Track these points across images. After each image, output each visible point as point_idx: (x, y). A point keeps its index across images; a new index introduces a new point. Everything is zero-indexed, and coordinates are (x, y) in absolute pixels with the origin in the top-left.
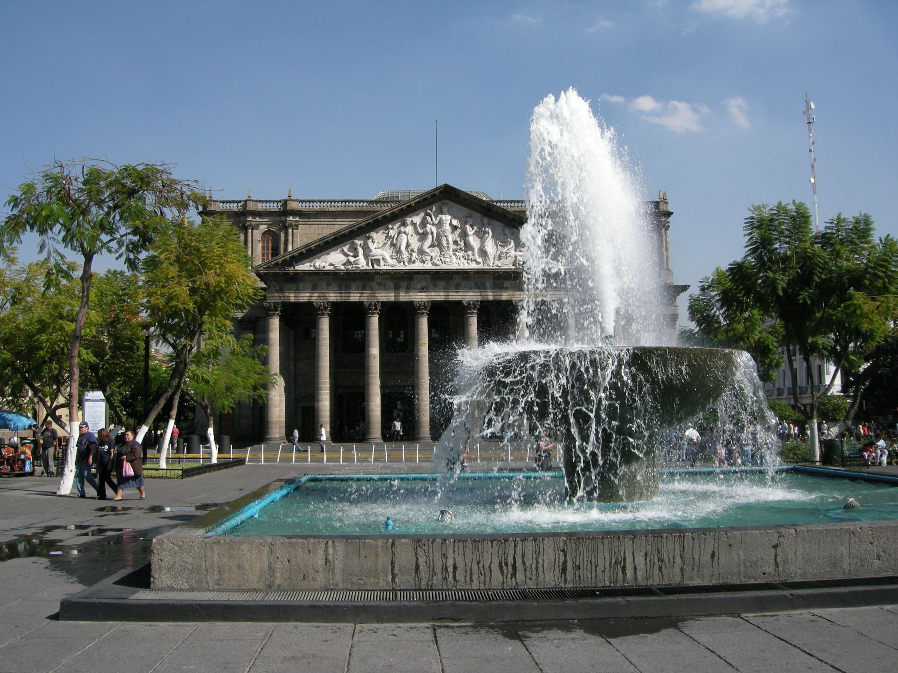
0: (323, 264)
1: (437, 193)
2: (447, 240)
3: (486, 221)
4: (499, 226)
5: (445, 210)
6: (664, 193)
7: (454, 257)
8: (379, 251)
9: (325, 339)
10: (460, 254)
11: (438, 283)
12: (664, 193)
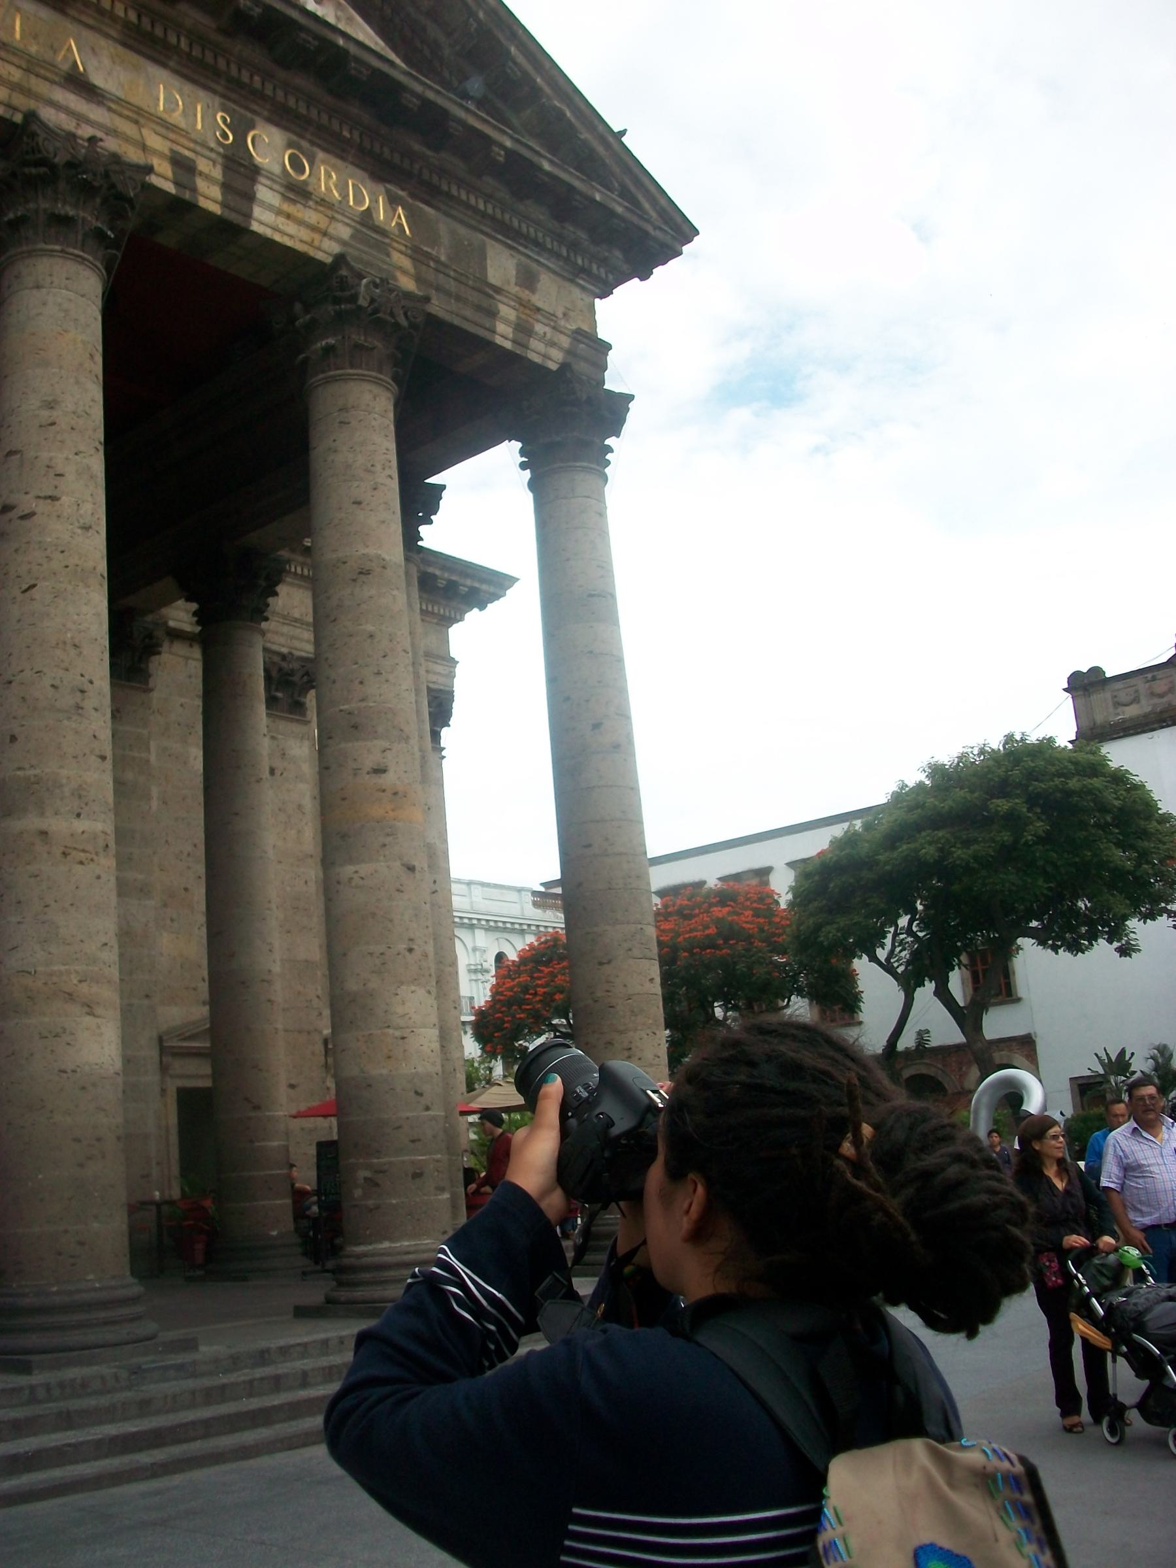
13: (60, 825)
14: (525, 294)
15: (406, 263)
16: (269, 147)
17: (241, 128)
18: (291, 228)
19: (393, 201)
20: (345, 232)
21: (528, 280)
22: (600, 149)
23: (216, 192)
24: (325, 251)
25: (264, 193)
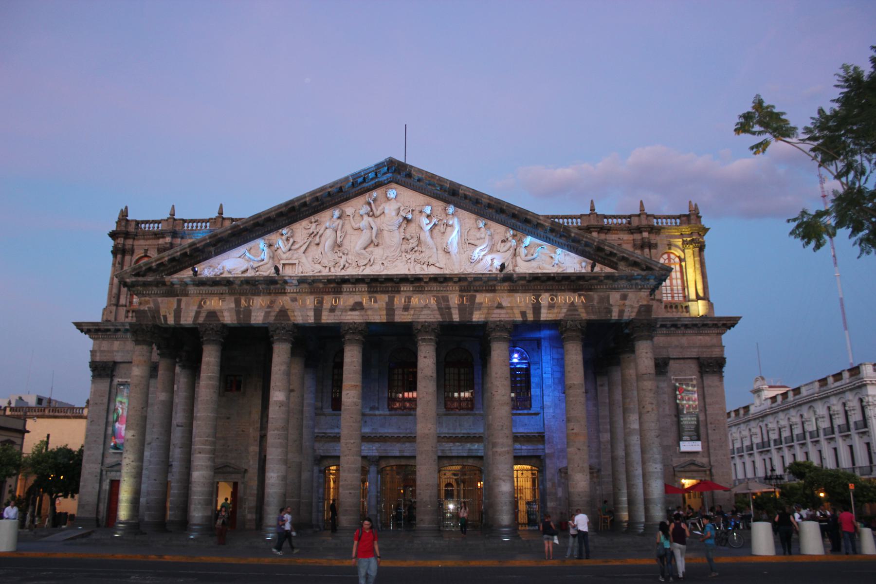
0: (217, 271)
3: (451, 209)
4: (469, 218)
7: (404, 259)
9: (210, 378)
10: (413, 256)
11: (378, 296)
12: (696, 205)
14: (622, 302)
15: (583, 310)
16: (545, 299)
17: (537, 299)
18: (551, 316)
19: (580, 296)
20: (564, 310)
21: (624, 297)
23: (532, 316)
24: (561, 316)
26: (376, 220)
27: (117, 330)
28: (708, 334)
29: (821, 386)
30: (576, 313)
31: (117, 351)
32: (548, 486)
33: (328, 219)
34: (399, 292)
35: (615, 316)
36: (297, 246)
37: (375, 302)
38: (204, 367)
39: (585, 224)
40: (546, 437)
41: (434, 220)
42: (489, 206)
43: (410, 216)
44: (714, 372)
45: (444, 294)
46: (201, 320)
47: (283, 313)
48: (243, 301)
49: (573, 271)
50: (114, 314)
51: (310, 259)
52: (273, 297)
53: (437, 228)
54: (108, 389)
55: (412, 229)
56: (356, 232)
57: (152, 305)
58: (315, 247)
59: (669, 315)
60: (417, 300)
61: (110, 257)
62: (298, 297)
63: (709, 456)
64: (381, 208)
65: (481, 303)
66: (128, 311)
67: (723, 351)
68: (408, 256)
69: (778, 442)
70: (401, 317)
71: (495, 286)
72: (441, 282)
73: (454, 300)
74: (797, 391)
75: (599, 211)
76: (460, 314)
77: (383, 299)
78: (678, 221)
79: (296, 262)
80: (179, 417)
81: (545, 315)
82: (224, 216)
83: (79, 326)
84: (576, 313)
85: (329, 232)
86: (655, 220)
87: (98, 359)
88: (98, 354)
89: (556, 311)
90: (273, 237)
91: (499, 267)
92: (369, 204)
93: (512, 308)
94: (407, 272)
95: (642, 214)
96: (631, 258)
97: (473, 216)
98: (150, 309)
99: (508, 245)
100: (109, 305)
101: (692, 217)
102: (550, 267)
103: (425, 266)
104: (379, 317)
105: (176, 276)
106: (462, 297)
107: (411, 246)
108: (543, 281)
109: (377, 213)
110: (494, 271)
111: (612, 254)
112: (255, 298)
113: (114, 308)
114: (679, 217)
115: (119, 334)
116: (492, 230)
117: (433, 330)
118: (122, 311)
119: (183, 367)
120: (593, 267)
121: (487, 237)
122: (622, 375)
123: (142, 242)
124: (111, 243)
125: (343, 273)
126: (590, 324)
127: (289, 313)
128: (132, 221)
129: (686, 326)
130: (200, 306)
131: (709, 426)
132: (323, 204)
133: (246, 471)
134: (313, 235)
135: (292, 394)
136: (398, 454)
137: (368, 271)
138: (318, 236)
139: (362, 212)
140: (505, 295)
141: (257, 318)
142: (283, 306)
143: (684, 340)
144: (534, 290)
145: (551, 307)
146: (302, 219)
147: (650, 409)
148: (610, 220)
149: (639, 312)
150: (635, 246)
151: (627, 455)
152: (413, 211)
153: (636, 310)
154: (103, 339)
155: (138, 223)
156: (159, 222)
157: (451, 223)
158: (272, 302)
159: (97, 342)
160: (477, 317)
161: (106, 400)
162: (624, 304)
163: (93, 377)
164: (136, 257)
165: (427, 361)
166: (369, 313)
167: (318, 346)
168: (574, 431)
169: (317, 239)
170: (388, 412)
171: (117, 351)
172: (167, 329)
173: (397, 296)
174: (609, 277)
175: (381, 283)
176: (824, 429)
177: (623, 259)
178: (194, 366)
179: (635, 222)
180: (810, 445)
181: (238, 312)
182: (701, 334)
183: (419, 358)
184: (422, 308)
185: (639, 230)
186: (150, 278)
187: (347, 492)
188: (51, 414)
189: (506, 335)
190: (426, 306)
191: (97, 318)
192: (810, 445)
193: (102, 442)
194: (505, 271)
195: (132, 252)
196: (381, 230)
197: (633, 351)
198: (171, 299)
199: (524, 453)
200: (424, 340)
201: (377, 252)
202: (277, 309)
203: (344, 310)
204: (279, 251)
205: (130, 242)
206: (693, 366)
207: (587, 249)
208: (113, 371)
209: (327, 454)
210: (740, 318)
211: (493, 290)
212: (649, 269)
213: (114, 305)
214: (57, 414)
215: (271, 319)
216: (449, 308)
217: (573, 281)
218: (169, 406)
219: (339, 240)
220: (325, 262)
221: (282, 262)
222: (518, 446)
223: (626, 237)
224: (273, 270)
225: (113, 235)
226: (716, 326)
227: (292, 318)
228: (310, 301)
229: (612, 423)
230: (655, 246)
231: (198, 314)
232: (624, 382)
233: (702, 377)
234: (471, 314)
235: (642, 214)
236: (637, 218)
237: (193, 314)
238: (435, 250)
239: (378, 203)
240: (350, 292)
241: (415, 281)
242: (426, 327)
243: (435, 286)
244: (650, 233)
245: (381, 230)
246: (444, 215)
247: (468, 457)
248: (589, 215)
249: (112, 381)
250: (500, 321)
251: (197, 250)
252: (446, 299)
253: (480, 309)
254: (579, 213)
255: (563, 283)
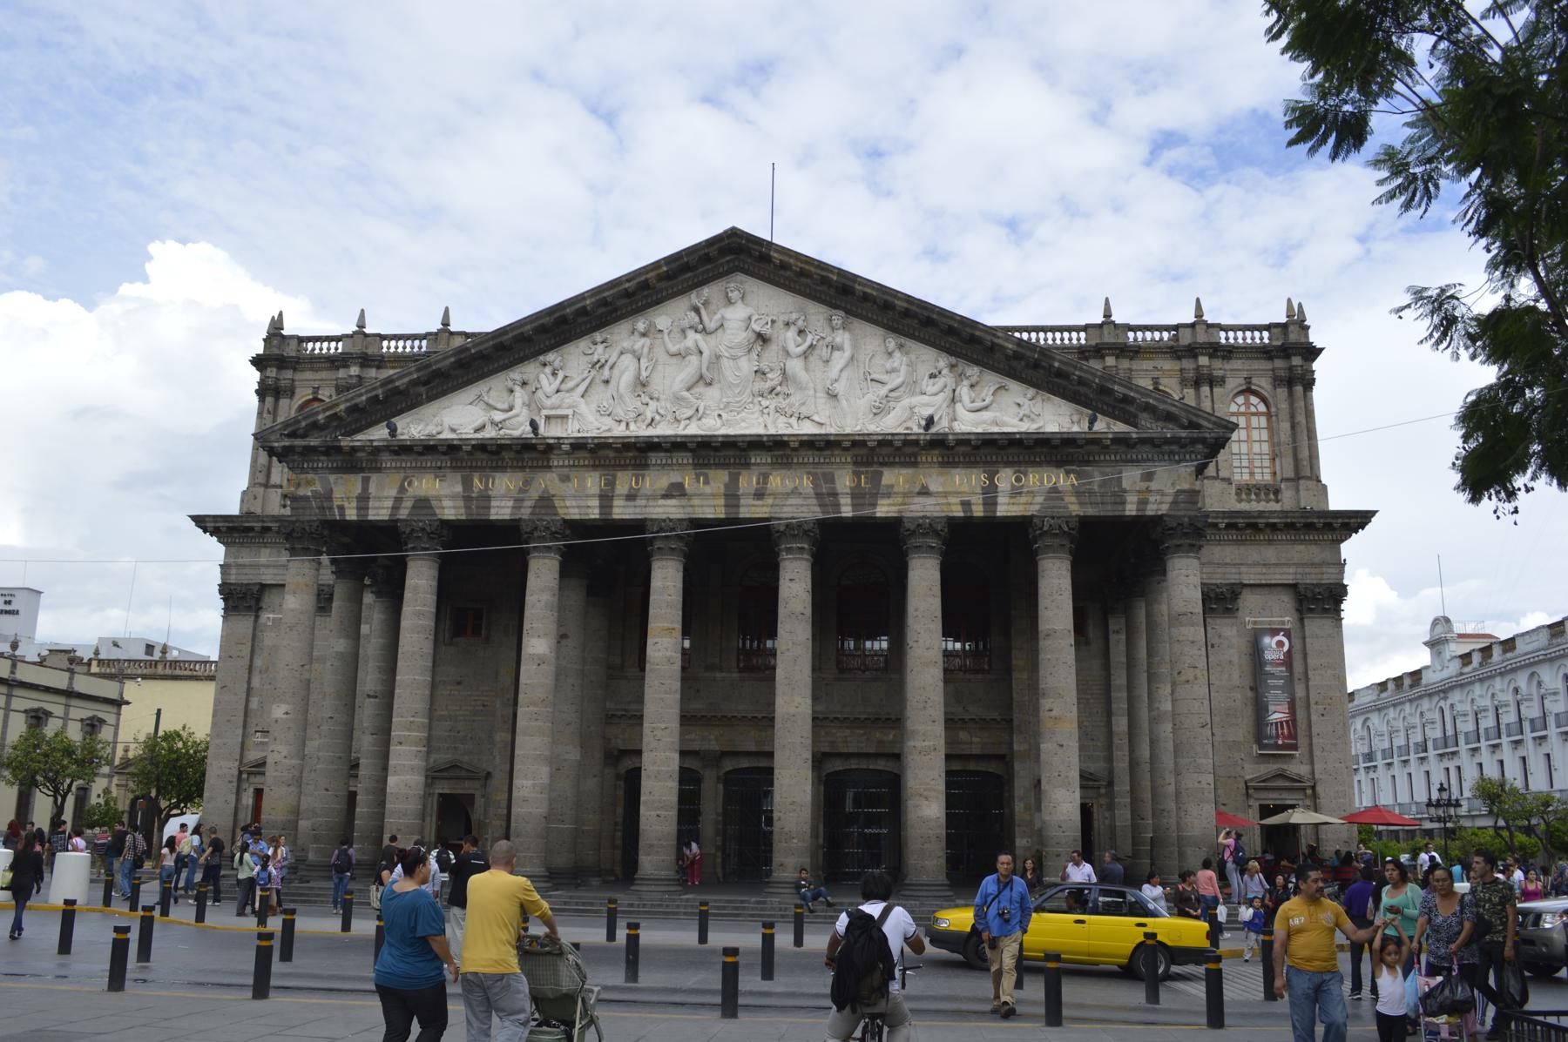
0: (431, 429)
1: (713, 251)
2: (739, 369)
3: (838, 317)
5: (734, 295)
6: (1300, 305)
7: (757, 408)
8: (569, 399)
9: (419, 615)
10: (771, 403)
11: (711, 473)
12: (1300, 305)
13: (919, 744)
14: (1144, 485)
15: (1074, 499)
16: (1006, 479)
17: (991, 479)
18: (1015, 508)
19: (1068, 473)
20: (1040, 499)
22: (1173, 409)
24: (1032, 510)
25: (1001, 500)
26: (708, 338)
27: (266, 530)
28: (1315, 542)
29: (1553, 636)
30: (1061, 504)
31: (268, 566)
32: (1017, 809)
33: (622, 336)
34: (747, 465)
35: (1131, 509)
36: (570, 384)
37: (706, 482)
38: (408, 595)
39: (1093, 343)
40: (1015, 723)
41: (810, 338)
42: (907, 313)
43: (767, 330)
44: (1326, 611)
45: (827, 469)
46: (403, 514)
47: (546, 501)
48: (476, 481)
49: (1056, 430)
50: (260, 500)
51: (594, 407)
52: (527, 474)
53: (817, 352)
54: (250, 631)
55: (771, 356)
56: (674, 360)
57: (318, 487)
58: (602, 387)
59: (1244, 506)
60: (777, 481)
61: (255, 399)
62: (572, 475)
63: (1312, 763)
64: (718, 316)
65: (892, 486)
66: (285, 496)
67: (1342, 572)
68: (765, 403)
69: (1406, 749)
70: (751, 509)
71: (915, 455)
72: (820, 449)
73: (844, 480)
74: (1509, 644)
75: (1118, 318)
76: (853, 505)
77: (719, 479)
78: (1266, 334)
79: (569, 412)
80: (369, 680)
81: (1005, 508)
82: (452, 328)
83: (200, 521)
84: (1057, 503)
85: (628, 360)
86: (1223, 334)
87: (233, 579)
88: (234, 571)
89: (1023, 499)
90: (529, 370)
91: (923, 423)
92: (697, 310)
93: (946, 494)
94: (761, 431)
95: (1199, 322)
96: (1162, 406)
97: (880, 331)
98: (316, 495)
99: (940, 382)
100: (253, 483)
101: (1291, 328)
102: (1015, 421)
103: (793, 421)
104: (711, 508)
105: (360, 437)
106: (857, 474)
107: (769, 384)
108: (1002, 448)
109: (711, 325)
110: (916, 430)
111: (1126, 400)
112: (498, 475)
113: (262, 490)
114: (1268, 327)
115: (269, 538)
116: (913, 357)
117: (806, 532)
118: (275, 497)
119: (379, 594)
120: (1092, 422)
121: (904, 369)
122: (1149, 615)
123: (308, 375)
124: (255, 375)
125: (651, 432)
126: (1086, 523)
127: (557, 503)
128: (292, 337)
129: (1273, 527)
130: (402, 489)
131: (1313, 707)
132: (616, 310)
133: (489, 775)
134: (598, 365)
135: (564, 642)
136: (753, 748)
137: (693, 429)
138: (607, 367)
139: (686, 323)
140: (934, 471)
141: (501, 511)
142: (546, 490)
143: (1270, 553)
144: (986, 463)
145: (1016, 493)
146: (579, 336)
147: (1191, 677)
148: (1140, 334)
149: (1175, 503)
150: (1183, 382)
151: (1154, 757)
152: (773, 322)
153: (1170, 499)
154: (242, 544)
155: (302, 340)
156: (337, 339)
157: (838, 340)
158: (526, 483)
159: (233, 549)
160: (884, 510)
161: (247, 651)
162: (1150, 489)
163: (225, 609)
164: (298, 401)
165: (795, 585)
166: (696, 502)
167: (607, 564)
168: (1053, 714)
169: (606, 373)
170: (736, 675)
171: (268, 566)
172: (342, 526)
173: (744, 472)
174: (1121, 441)
175: (716, 449)
176: (1557, 715)
177: (1147, 408)
178: (393, 591)
179: (1186, 338)
180: (1530, 744)
181: (467, 499)
182: (1303, 542)
183: (782, 581)
184: (787, 498)
185: (1192, 351)
186: (313, 442)
187: (654, 813)
188: (168, 672)
189: (933, 542)
190: (795, 492)
191: (233, 509)
192: (1530, 744)
193: (241, 724)
194: (933, 430)
195: (291, 392)
196: (718, 357)
197: (1164, 573)
198: (352, 477)
199: (975, 752)
200: (789, 550)
201: (711, 396)
202: (535, 493)
203: (653, 497)
204: (539, 393)
205: (288, 374)
206: (1286, 601)
207: (1082, 389)
208: (258, 600)
209: (630, 747)
210: (1373, 513)
211: (914, 464)
212: (1193, 425)
213: (261, 485)
214: (178, 672)
215: (525, 513)
216: (835, 495)
217: (1056, 447)
218: (352, 662)
219: (644, 374)
220: (620, 412)
221: (544, 412)
222: (963, 735)
223: (1168, 365)
224: (529, 428)
225: (257, 362)
226: (1329, 527)
227: (561, 511)
228: (592, 482)
229: (1131, 700)
230: (1222, 381)
231: (398, 500)
232: (1151, 626)
233: (1302, 620)
234: (874, 505)
235: (1199, 322)
236: (1188, 330)
237: (389, 503)
238: (811, 392)
239: (712, 307)
240: (663, 466)
241: (777, 449)
242: (796, 530)
243: (809, 456)
244: (1211, 357)
245: (718, 357)
246: (828, 330)
247: (877, 756)
248: (1100, 326)
249: (257, 617)
250: (925, 517)
251: (397, 392)
252: (830, 479)
253: (888, 495)
254: (1083, 323)
255: (1038, 450)
